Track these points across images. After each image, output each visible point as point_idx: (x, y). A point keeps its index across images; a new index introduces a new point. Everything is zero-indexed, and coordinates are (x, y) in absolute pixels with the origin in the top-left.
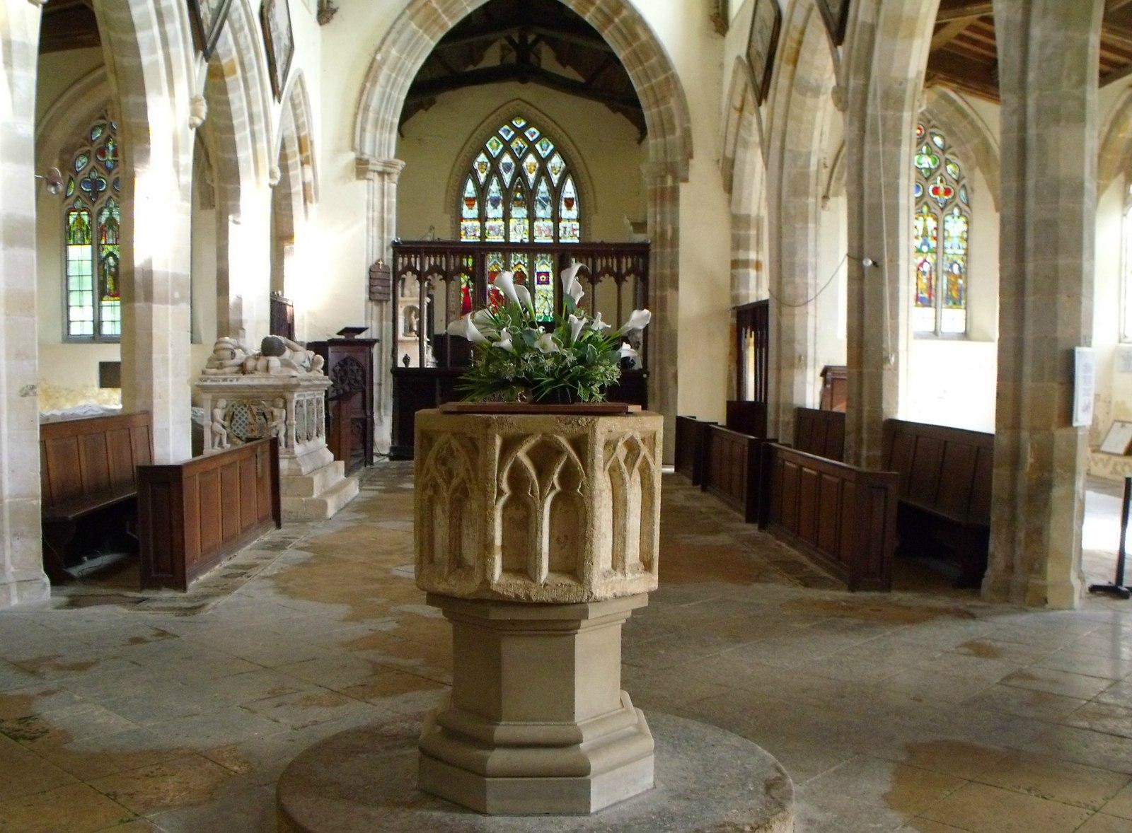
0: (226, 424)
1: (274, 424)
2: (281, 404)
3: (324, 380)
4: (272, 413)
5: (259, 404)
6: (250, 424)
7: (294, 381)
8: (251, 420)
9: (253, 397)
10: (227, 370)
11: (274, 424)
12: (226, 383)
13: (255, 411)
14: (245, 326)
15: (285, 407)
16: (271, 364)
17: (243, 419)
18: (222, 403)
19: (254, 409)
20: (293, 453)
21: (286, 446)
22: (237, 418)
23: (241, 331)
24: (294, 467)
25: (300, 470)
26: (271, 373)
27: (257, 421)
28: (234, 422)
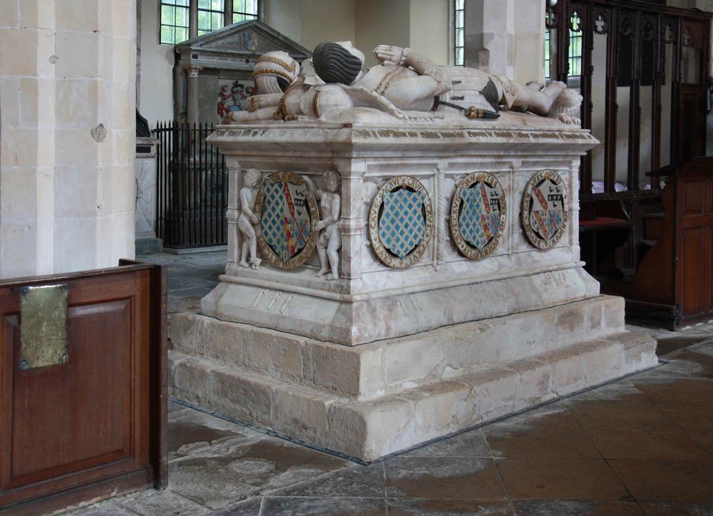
0: (255, 218)
1: (321, 224)
2: (333, 186)
3: (583, 137)
4: (319, 201)
5: (299, 182)
6: (286, 221)
7: (342, 136)
8: (287, 214)
9: (288, 168)
10: (260, 113)
11: (321, 224)
12: (250, 138)
13: (293, 196)
14: (489, 46)
15: (338, 191)
16: (322, 101)
17: (278, 211)
18: (253, 176)
19: (292, 189)
20: (348, 291)
21: (340, 274)
22: (269, 209)
23: (481, 55)
24: (342, 320)
25: (348, 331)
26: (323, 119)
27: (296, 213)
28: (265, 216)
